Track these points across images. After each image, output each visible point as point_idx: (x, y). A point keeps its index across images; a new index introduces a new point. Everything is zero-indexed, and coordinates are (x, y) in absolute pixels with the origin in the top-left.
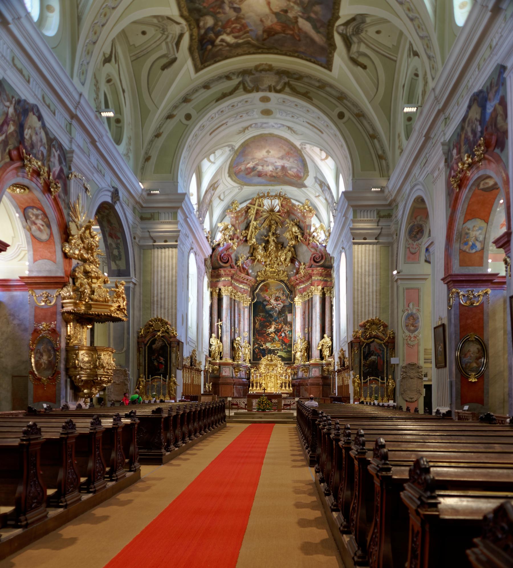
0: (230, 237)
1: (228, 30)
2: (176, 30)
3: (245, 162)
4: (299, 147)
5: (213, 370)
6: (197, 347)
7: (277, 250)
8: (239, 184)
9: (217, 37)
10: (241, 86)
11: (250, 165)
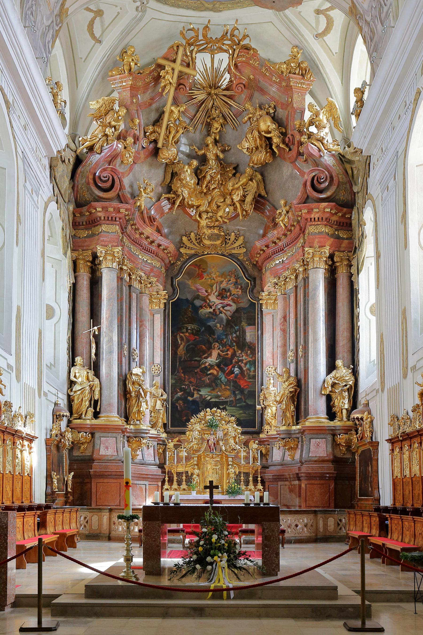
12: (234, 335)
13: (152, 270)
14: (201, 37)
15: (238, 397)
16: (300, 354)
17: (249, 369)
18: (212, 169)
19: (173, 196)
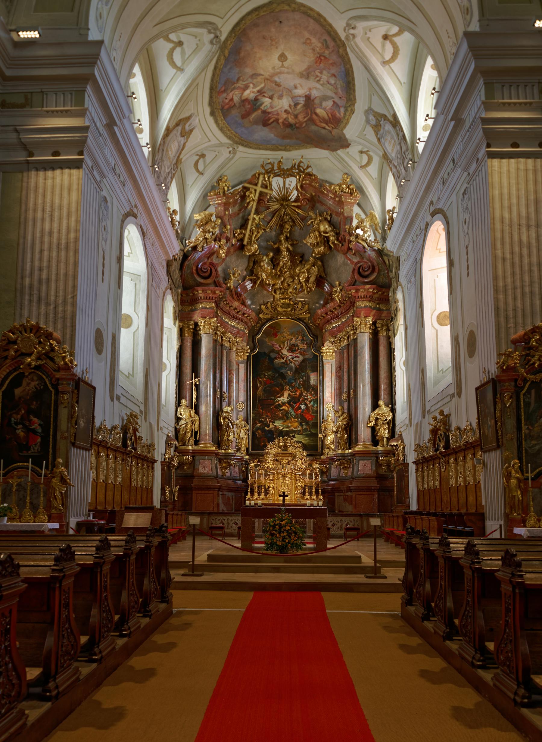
0: (214, 237)
5: (181, 464)
7: (294, 265)
8: (229, 138)
12: (301, 380)
13: (238, 332)
14: (276, 168)
15: (304, 427)
16: (352, 396)
17: (313, 406)
18: (285, 258)
19: (255, 277)
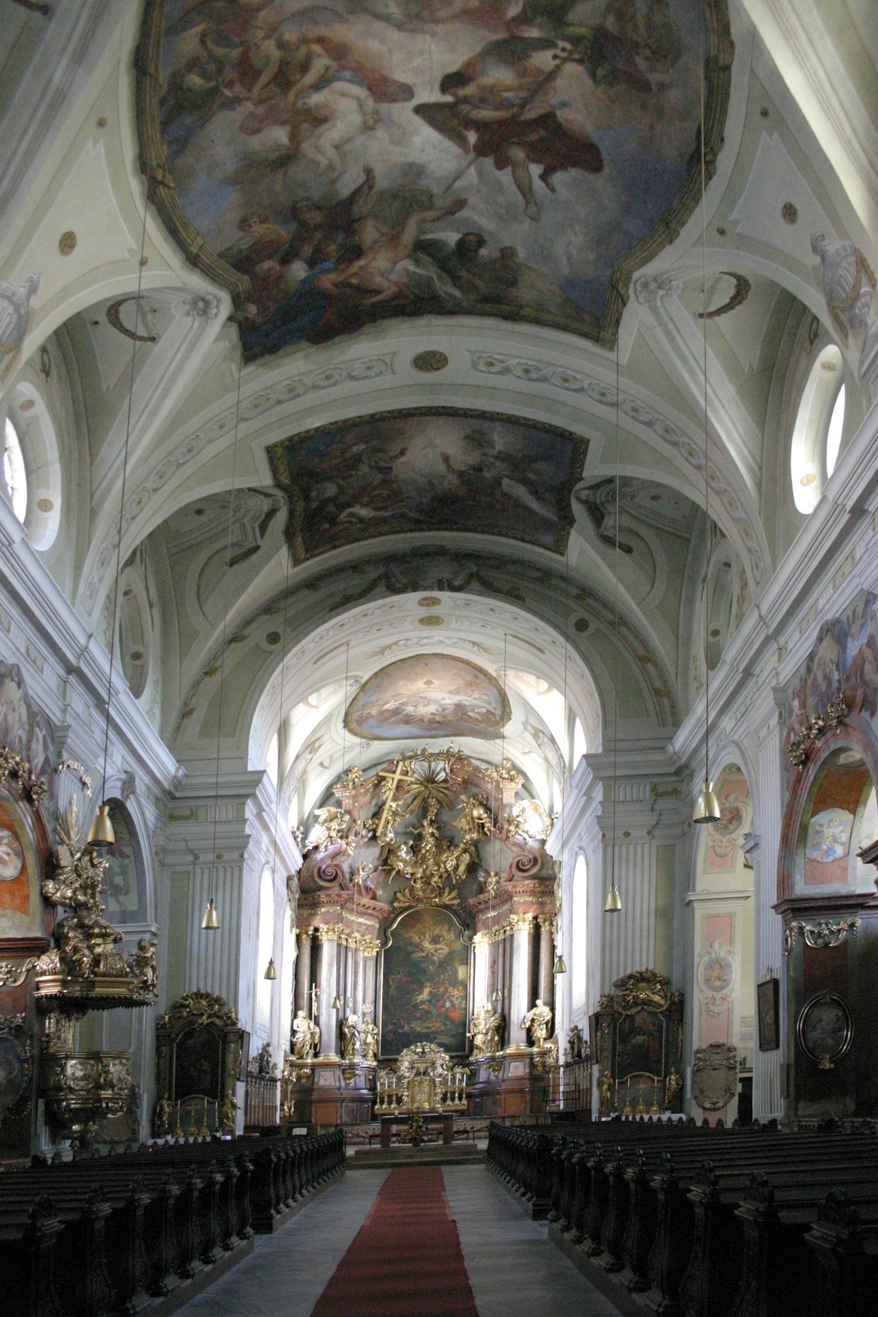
1: (365, 500)
2: (266, 505)
3: (380, 702)
4: (494, 674)
5: (299, 1078)
6: (271, 1036)
9: (341, 512)
10: (383, 582)
11: (391, 705)
